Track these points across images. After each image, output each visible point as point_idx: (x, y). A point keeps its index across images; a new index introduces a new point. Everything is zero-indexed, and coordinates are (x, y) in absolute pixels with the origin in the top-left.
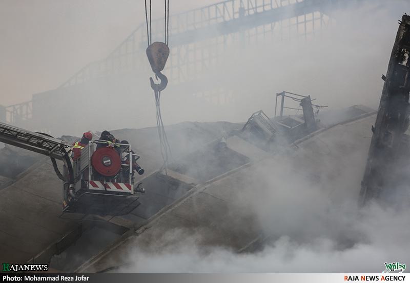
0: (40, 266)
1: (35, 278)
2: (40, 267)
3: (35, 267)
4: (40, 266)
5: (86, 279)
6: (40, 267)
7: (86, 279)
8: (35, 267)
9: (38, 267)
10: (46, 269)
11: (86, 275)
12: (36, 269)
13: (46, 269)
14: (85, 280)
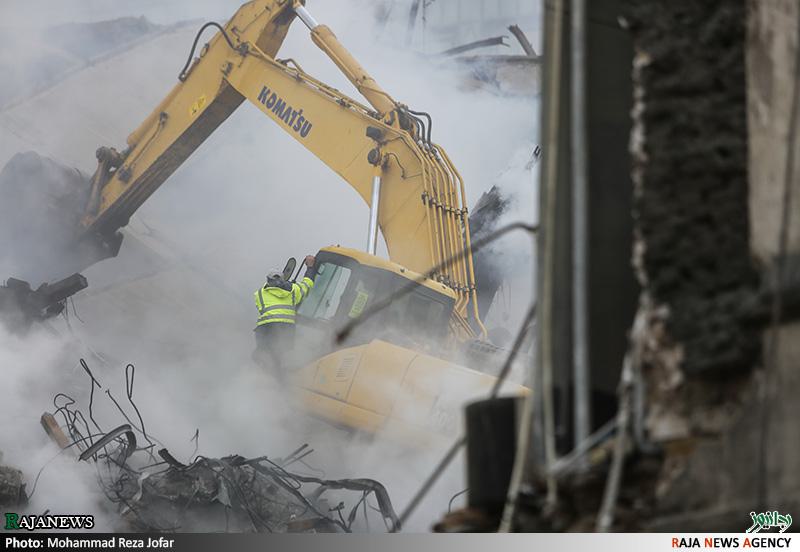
0: (77, 518)
1: (67, 543)
2: (78, 521)
3: (68, 522)
4: (77, 518)
5: (168, 544)
6: (78, 521)
7: (168, 544)
8: (68, 522)
9: (74, 520)
10: (89, 524)
11: (167, 537)
12: (71, 524)
13: (89, 524)
14: (165, 546)
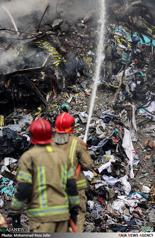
0: (23, 228)
1: (20, 235)
2: (23, 229)
3: (20, 229)
4: (23, 228)
5: (49, 236)
6: (23, 229)
7: (49, 236)
8: (20, 229)
9: (22, 229)
10: (26, 230)
11: (49, 234)
12: (21, 230)
13: (26, 230)
14: (48, 236)
